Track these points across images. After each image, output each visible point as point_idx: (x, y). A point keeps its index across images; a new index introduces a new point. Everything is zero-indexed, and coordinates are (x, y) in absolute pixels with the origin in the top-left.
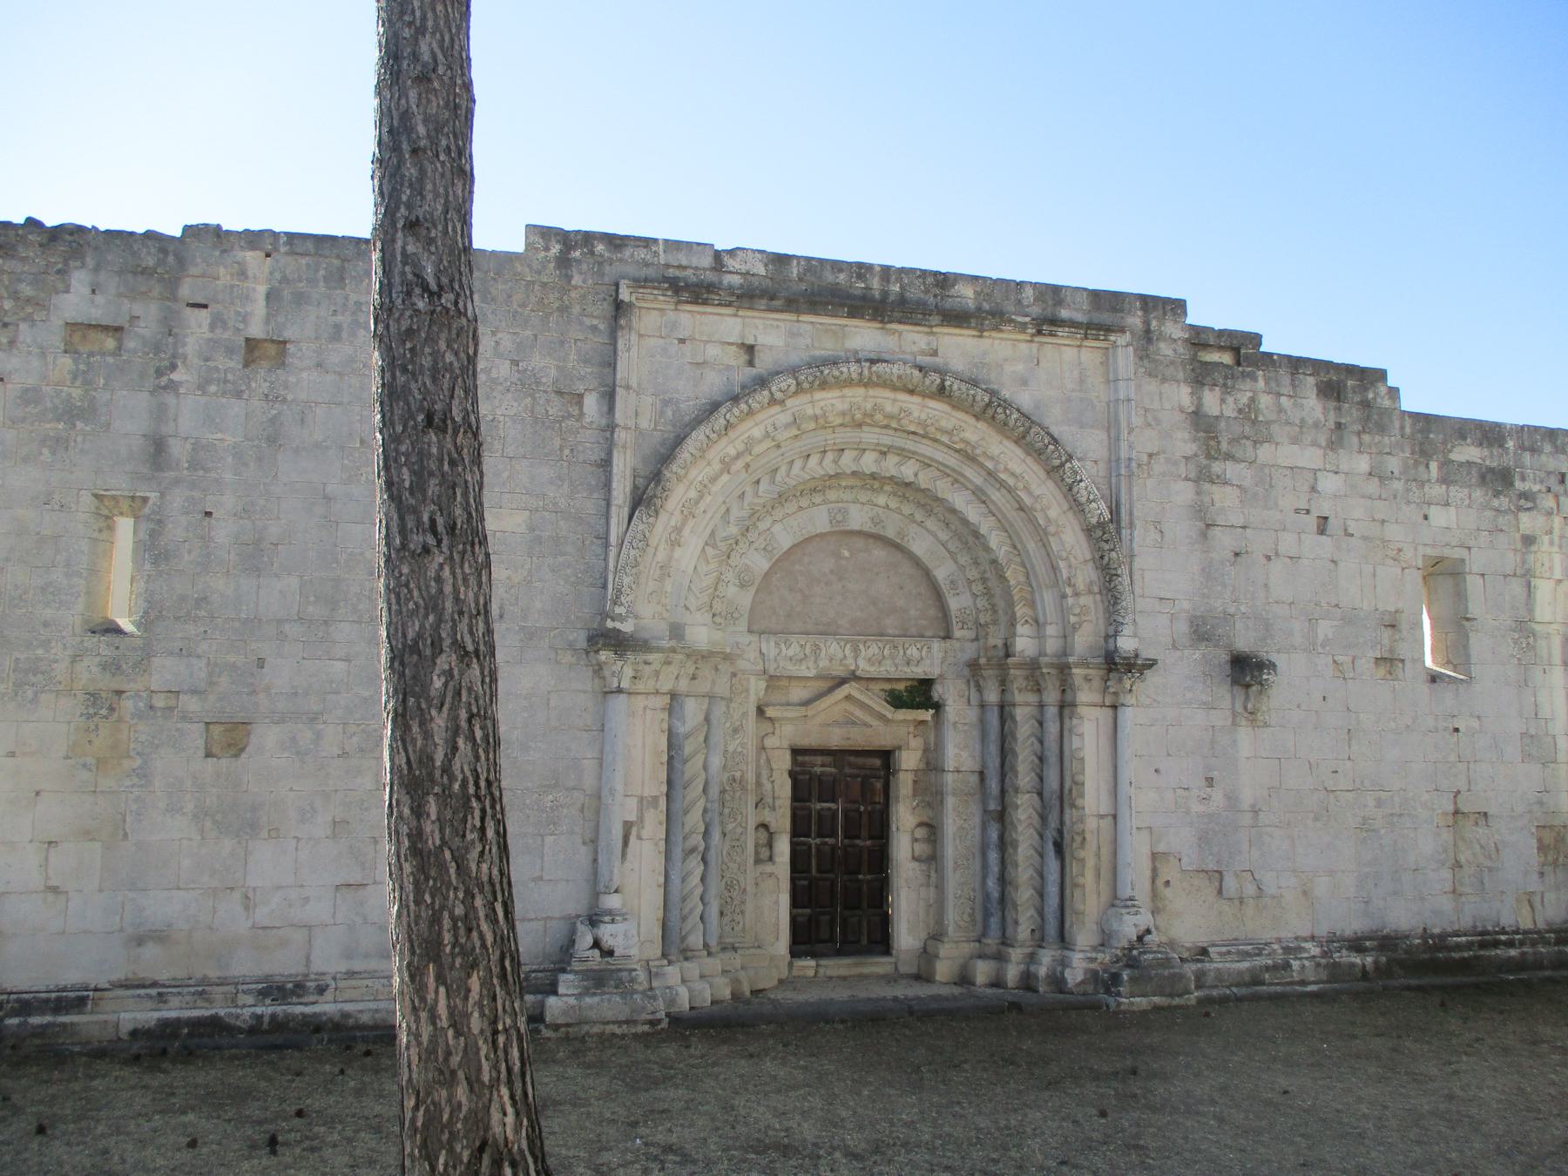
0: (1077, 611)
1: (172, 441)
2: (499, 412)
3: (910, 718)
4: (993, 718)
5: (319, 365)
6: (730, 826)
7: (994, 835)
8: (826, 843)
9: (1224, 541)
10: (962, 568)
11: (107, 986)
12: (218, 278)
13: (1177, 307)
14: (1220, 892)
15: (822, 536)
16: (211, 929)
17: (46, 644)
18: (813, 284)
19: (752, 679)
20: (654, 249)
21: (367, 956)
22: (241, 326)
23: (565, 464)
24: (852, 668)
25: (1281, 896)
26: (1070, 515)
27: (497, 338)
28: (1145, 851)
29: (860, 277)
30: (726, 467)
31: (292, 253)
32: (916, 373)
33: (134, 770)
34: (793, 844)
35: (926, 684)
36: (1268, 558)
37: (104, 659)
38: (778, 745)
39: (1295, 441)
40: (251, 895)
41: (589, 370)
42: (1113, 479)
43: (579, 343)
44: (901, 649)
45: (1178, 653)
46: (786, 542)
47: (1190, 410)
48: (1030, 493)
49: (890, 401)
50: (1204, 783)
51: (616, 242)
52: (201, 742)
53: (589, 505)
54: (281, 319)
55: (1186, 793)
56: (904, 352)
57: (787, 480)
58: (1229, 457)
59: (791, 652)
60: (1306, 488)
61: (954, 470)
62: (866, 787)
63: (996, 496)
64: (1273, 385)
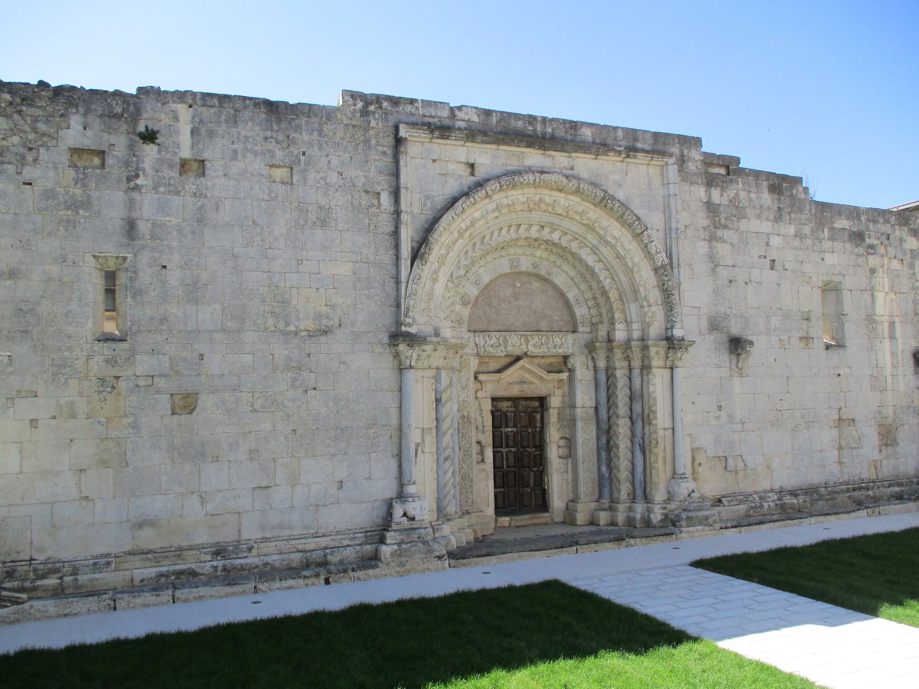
0: (650, 315)
1: (139, 222)
2: (332, 203)
3: (556, 378)
4: (602, 377)
5: (225, 175)
6: (463, 444)
7: (604, 441)
8: (511, 451)
9: (724, 273)
10: (582, 292)
11: (122, 554)
12: (161, 121)
13: (697, 142)
14: (726, 468)
15: (505, 275)
16: (181, 517)
17: (70, 349)
18: (504, 127)
19: (472, 358)
20: (416, 105)
21: (273, 528)
22: (177, 150)
23: (372, 234)
24: (525, 350)
25: (756, 468)
26: (645, 260)
27: (328, 159)
28: (688, 447)
29: (530, 123)
30: (461, 234)
31: (204, 105)
32: (565, 180)
33: (129, 424)
34: (494, 453)
35: (566, 358)
36: (746, 283)
37: (107, 357)
38: (484, 396)
39: (758, 217)
40: (203, 496)
41: (382, 178)
42: (668, 241)
43: (376, 162)
44: (551, 338)
46: (486, 279)
47: (705, 201)
48: (624, 249)
49: (548, 196)
50: (716, 409)
51: (396, 101)
52: (169, 406)
53: (387, 258)
54: (201, 147)
56: (555, 168)
57: (490, 242)
58: (725, 227)
59: (492, 342)
60: (764, 244)
61: (580, 235)
62: (532, 419)
63: (604, 250)
64: (747, 186)
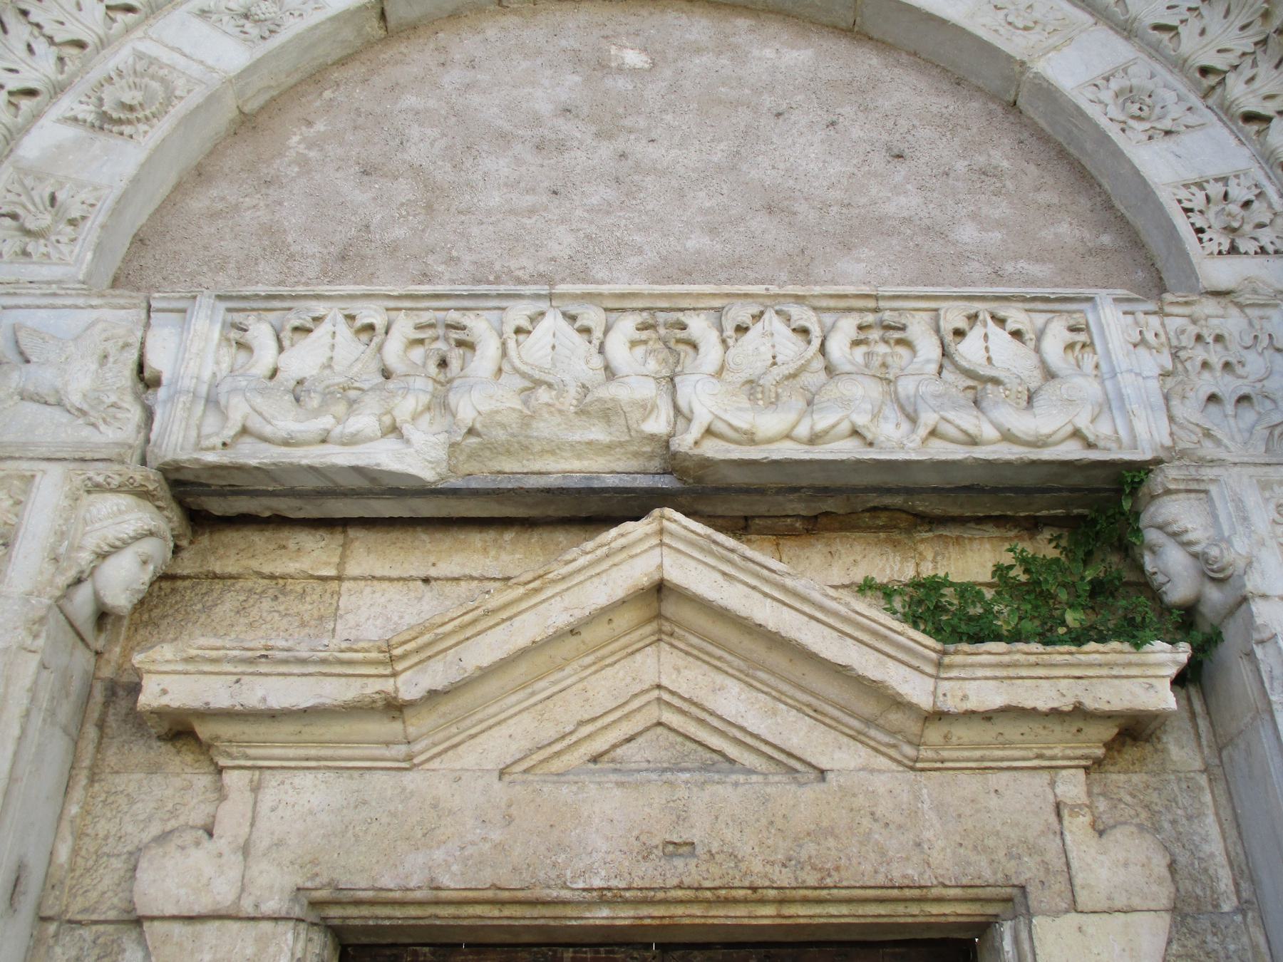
3: (1042, 696)
24: (658, 424)
38: (222, 893)
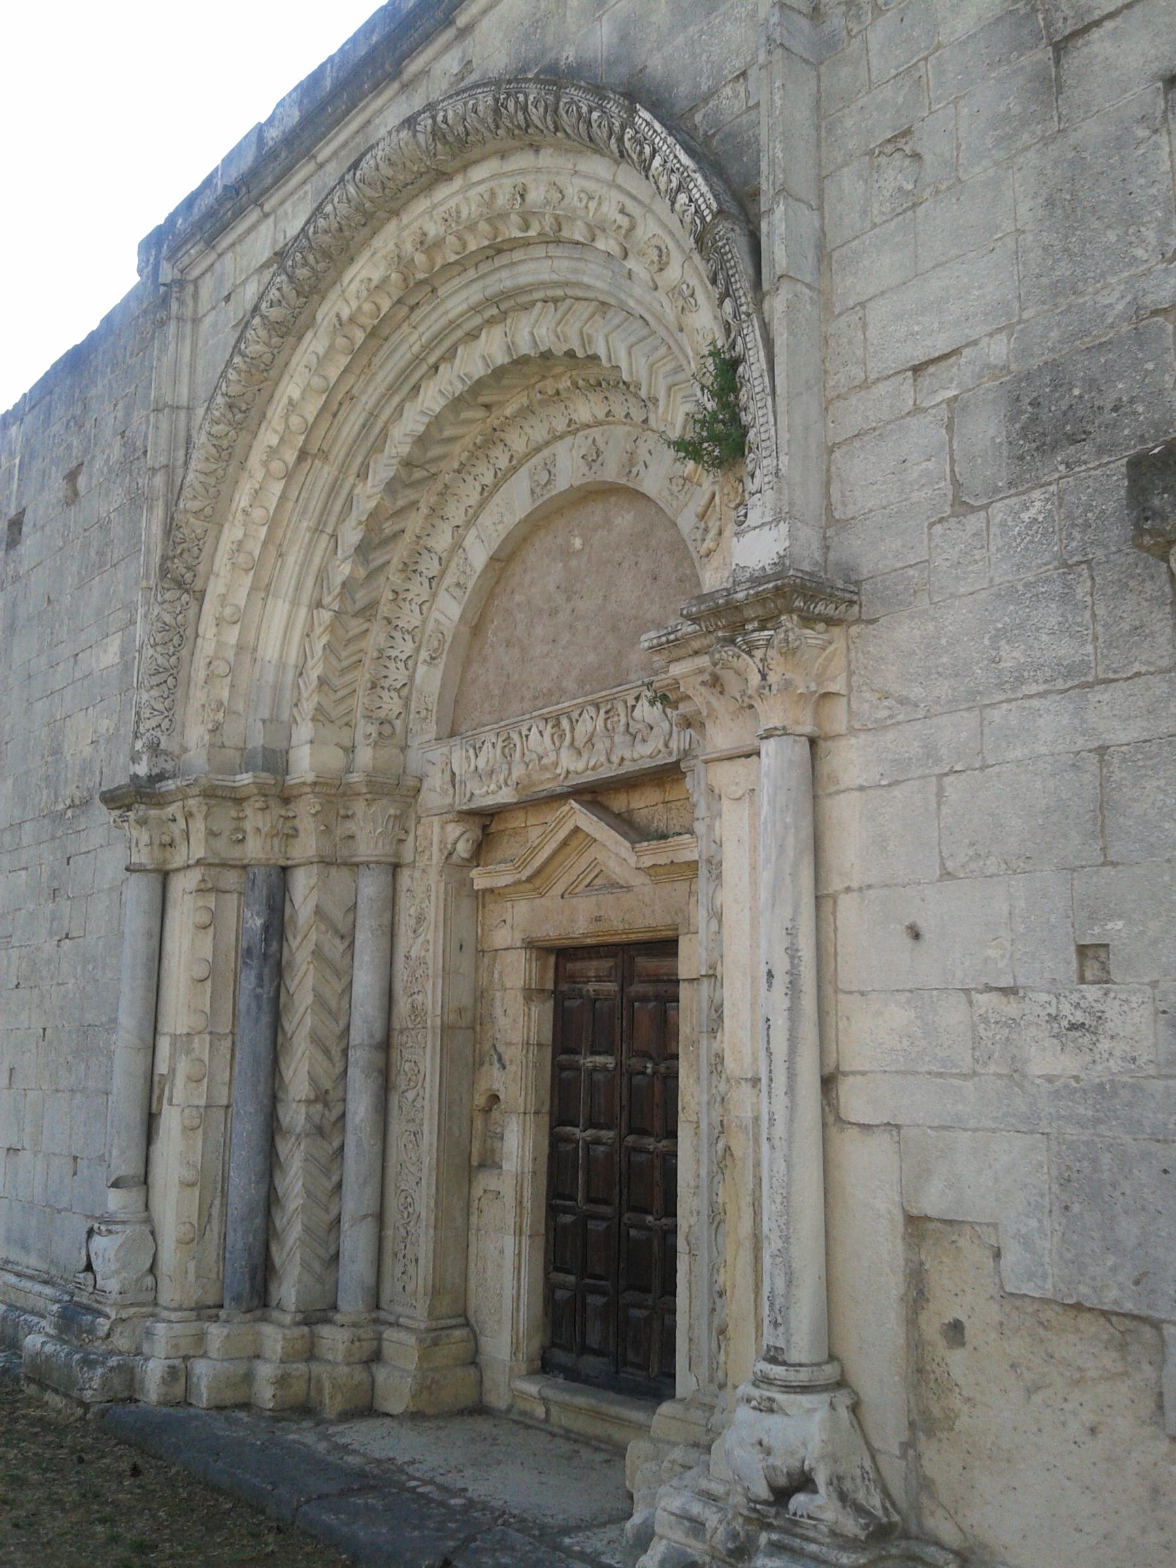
45: (974, 522)
55: (1011, 1008)
